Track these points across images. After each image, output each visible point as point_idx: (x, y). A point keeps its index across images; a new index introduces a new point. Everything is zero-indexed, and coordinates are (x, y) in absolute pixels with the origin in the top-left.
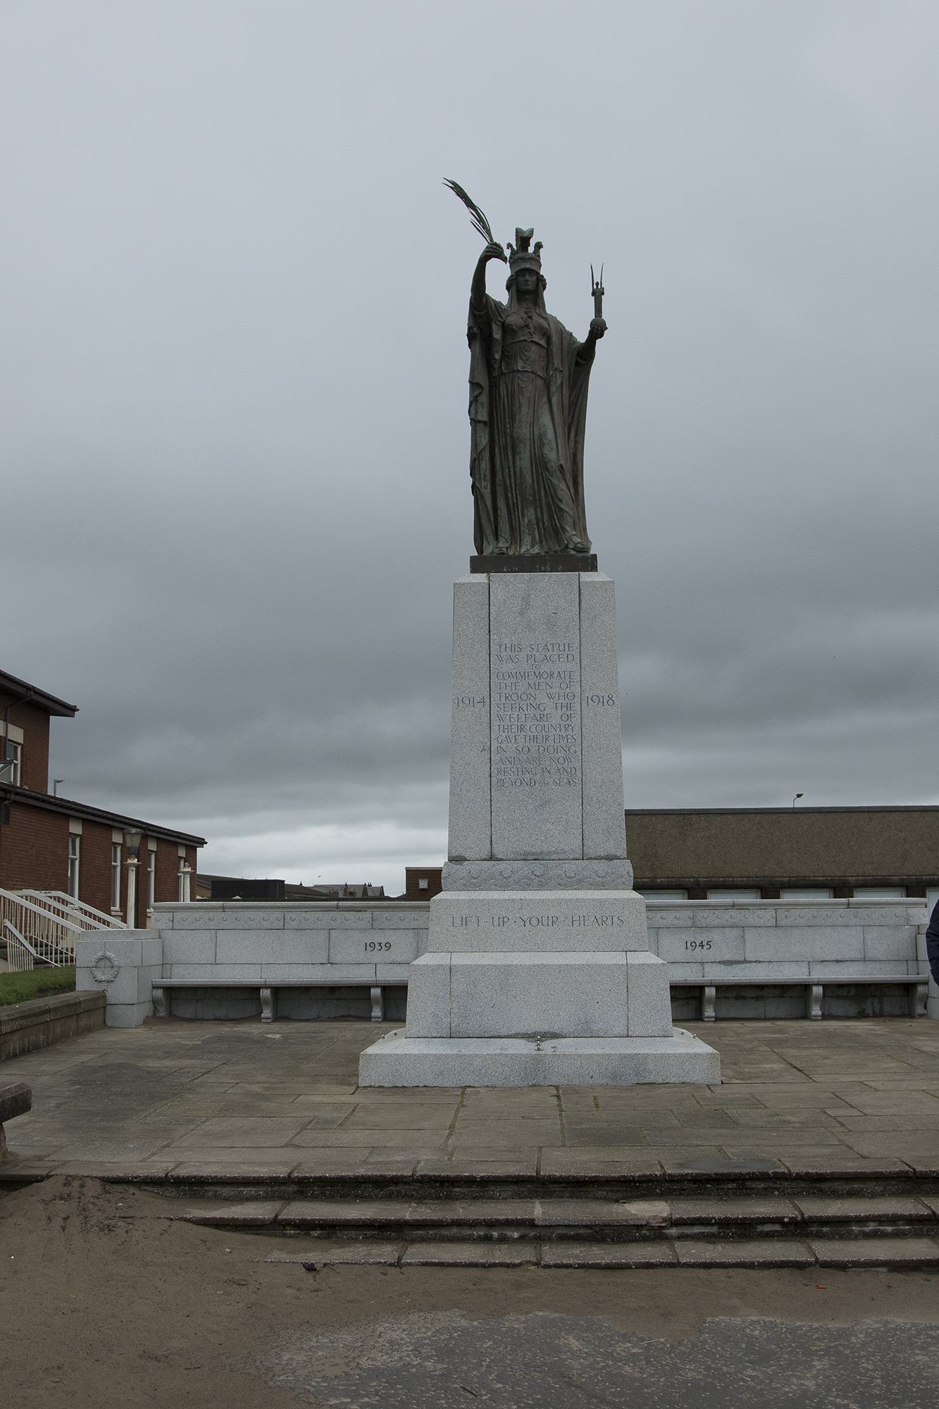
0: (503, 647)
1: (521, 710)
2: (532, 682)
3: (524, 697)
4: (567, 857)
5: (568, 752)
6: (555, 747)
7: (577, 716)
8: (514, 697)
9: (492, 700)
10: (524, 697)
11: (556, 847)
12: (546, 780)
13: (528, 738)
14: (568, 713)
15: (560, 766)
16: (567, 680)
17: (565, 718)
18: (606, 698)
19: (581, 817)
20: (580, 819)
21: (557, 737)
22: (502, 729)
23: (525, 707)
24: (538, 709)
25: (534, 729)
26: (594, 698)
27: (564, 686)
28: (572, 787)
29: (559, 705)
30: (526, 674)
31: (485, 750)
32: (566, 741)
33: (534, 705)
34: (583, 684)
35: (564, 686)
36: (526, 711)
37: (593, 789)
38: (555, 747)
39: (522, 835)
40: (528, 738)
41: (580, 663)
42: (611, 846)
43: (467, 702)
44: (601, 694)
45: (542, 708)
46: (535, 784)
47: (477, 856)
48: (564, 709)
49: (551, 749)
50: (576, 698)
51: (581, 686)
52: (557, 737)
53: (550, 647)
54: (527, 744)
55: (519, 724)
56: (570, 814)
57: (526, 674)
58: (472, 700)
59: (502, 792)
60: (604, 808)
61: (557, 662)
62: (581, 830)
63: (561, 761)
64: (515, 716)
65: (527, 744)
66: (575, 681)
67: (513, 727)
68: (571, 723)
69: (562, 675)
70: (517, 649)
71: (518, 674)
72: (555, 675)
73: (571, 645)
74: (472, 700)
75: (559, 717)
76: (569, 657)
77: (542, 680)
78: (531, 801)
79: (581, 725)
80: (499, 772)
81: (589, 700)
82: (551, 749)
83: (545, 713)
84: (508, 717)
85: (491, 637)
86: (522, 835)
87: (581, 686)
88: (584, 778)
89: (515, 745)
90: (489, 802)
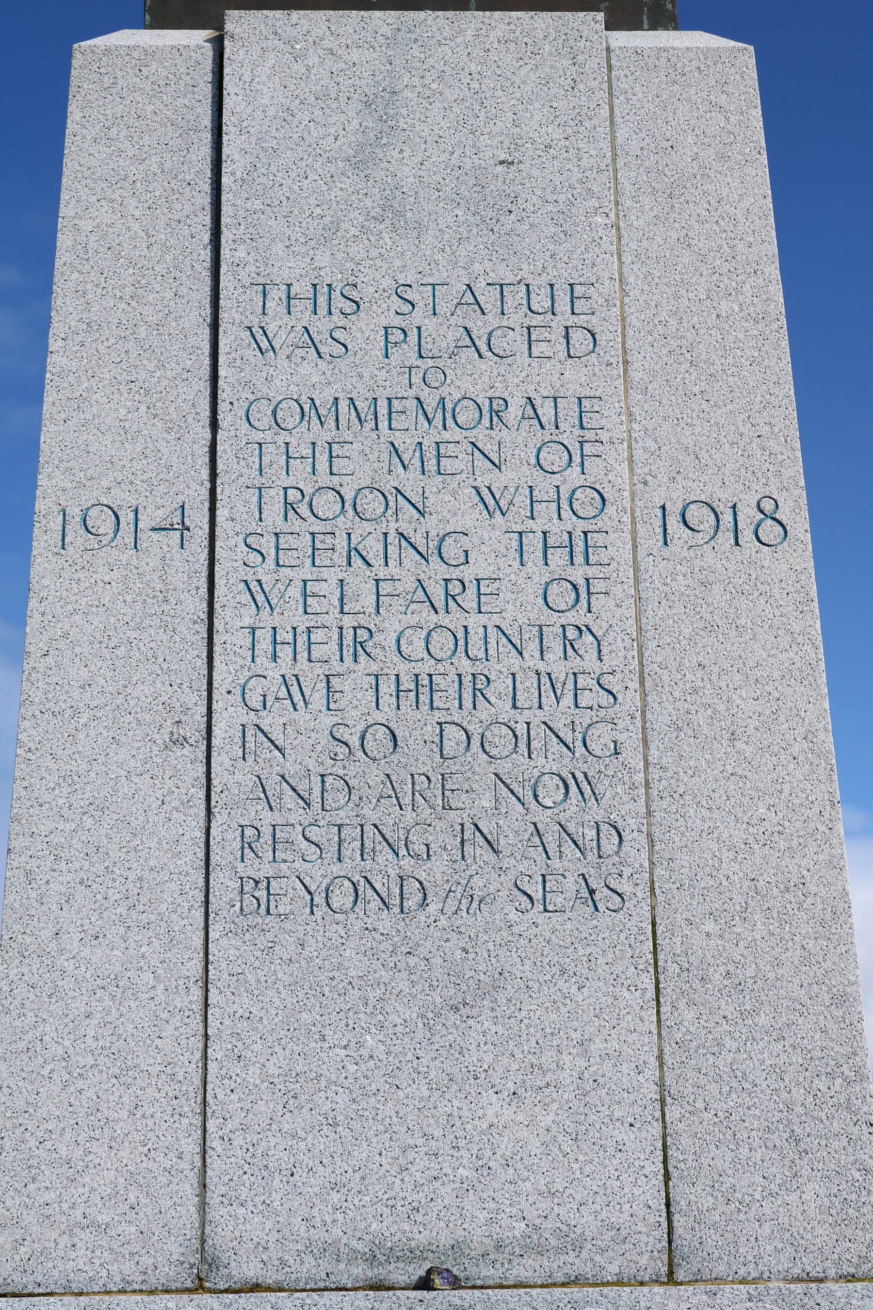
0: (277, 294)
1: (357, 561)
2: (406, 442)
3: (372, 504)
4: (588, 1270)
5: (580, 750)
6: (521, 729)
7: (617, 590)
8: (326, 504)
9: (222, 514)
10: (372, 504)
11: (532, 1215)
12: (477, 882)
13: (387, 688)
14: (578, 575)
15: (543, 818)
16: (570, 436)
17: (561, 596)
18: (748, 515)
19: (653, 1062)
20: (652, 1073)
21: (525, 684)
22: (264, 644)
23: (373, 548)
24: (434, 559)
25: (417, 649)
26: (695, 514)
27: (553, 457)
28: (605, 919)
29: (533, 543)
30: (383, 411)
31: (179, 742)
32: (568, 700)
33: (419, 540)
34: (638, 454)
35: (553, 457)
36: (378, 562)
37: (710, 926)
38: (521, 729)
39: (362, 1153)
40: (387, 688)
41: (626, 362)
42: (812, 1211)
43: (106, 526)
44: (723, 497)
45: (451, 550)
46: (424, 903)
47: (128, 1268)
48: (558, 558)
49: (500, 738)
50: (610, 510)
51: (631, 459)
52: (525, 684)
53: (489, 298)
54: (388, 713)
55: (348, 622)
56: (598, 1045)
57: (383, 411)
58: (127, 517)
59: (263, 941)
60: (763, 1019)
61: (523, 359)
62: (656, 1129)
63: (551, 793)
64: (330, 588)
65: (388, 713)
66: (604, 436)
67: (318, 636)
68: (589, 619)
69: (546, 411)
70: (339, 303)
71: (343, 405)
72: (513, 413)
73: (579, 290)
74: (127, 517)
75: (532, 592)
76: (577, 336)
77: (453, 434)
78: (403, 986)
79: (640, 629)
80: (247, 846)
81: (674, 523)
82: (500, 738)
83: (468, 573)
84: (295, 591)
85: (225, 253)
86: (362, 1153)
87: (631, 459)
88: (659, 871)
89: (328, 720)
90: (196, 993)
